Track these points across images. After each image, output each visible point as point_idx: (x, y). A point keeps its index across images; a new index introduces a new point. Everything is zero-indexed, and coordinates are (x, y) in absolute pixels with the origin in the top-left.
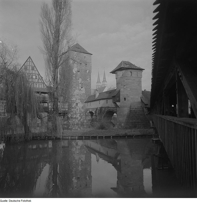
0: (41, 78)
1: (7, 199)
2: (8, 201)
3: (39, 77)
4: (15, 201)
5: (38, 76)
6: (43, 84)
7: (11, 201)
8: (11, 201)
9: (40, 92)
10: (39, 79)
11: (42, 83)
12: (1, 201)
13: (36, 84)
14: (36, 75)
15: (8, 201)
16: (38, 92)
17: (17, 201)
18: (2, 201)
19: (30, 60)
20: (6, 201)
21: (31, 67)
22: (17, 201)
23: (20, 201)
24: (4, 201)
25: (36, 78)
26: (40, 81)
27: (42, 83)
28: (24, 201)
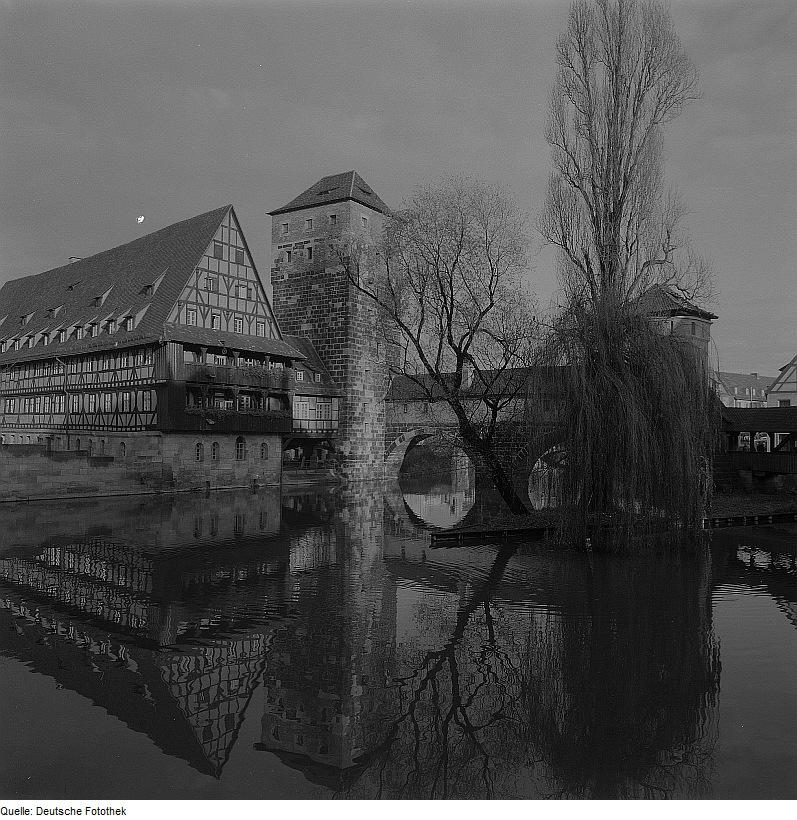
0: (263, 300)
1: (30, 804)
2: (34, 812)
4: (61, 812)
5: (253, 289)
7: (46, 812)
8: (46, 812)
9: (267, 354)
11: (266, 317)
12: (4, 811)
14: (251, 285)
15: (31, 812)
16: (260, 356)
17: (68, 812)
18: (7, 813)
19: (232, 221)
20: (26, 812)
21: (233, 250)
22: (68, 812)
23: (79, 811)
24: (17, 811)
25: (249, 298)
26: (261, 312)
27: (266, 317)
28: (97, 812)
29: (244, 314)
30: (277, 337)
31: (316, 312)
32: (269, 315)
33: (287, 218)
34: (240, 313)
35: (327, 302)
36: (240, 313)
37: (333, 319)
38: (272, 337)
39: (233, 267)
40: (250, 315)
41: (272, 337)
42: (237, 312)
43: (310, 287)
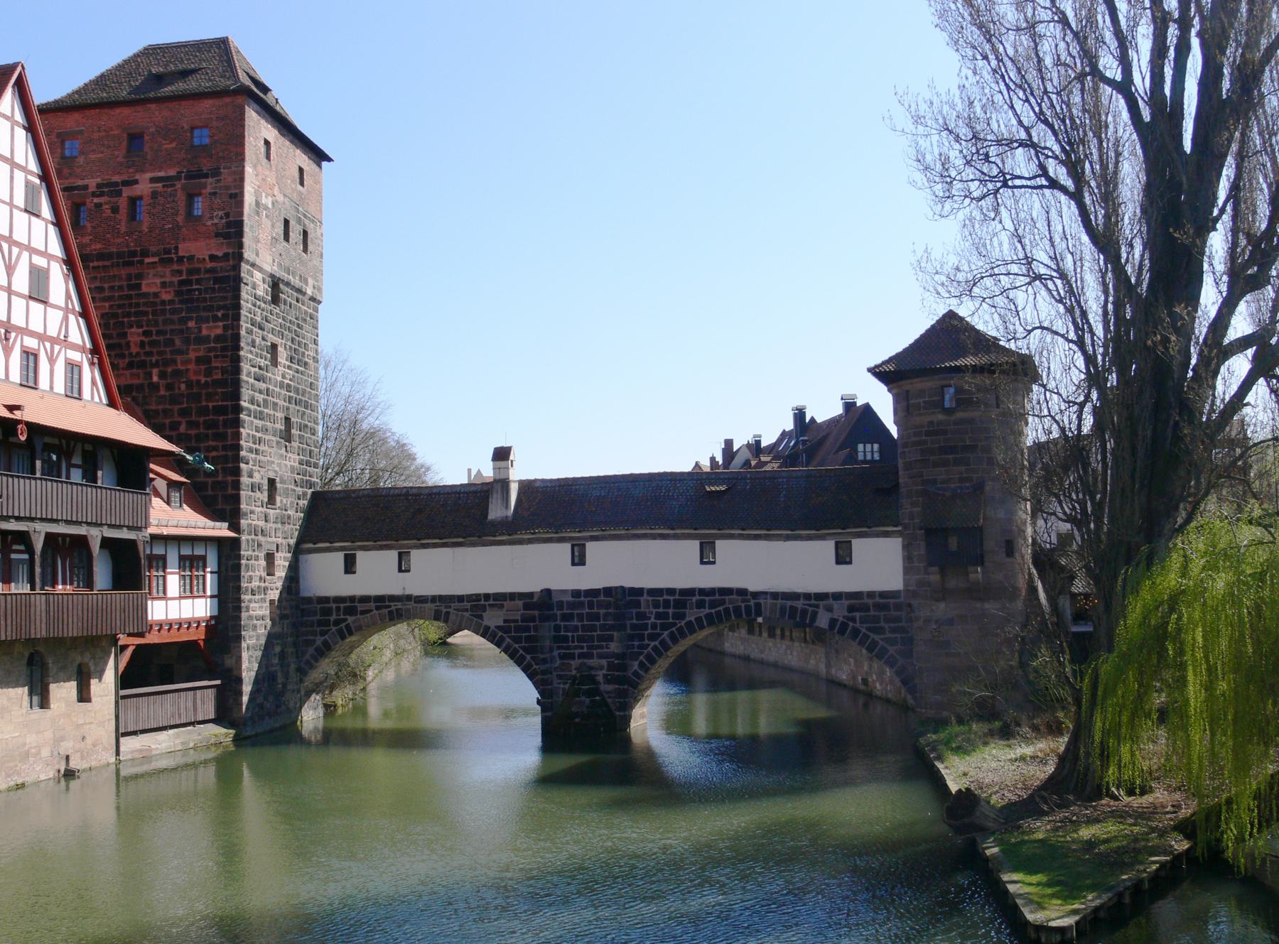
0: (78, 308)
3: (68, 296)
6: (92, 364)
10: (67, 311)
13: (52, 361)
29: (42, 337)
30: (105, 401)
31: (152, 343)
32: (89, 345)
33: (72, 122)
34: (33, 334)
35: (184, 321)
36: (33, 334)
37: (199, 361)
38: (97, 399)
39: (21, 218)
40: (54, 341)
41: (97, 399)
42: (25, 331)
43: (139, 286)
